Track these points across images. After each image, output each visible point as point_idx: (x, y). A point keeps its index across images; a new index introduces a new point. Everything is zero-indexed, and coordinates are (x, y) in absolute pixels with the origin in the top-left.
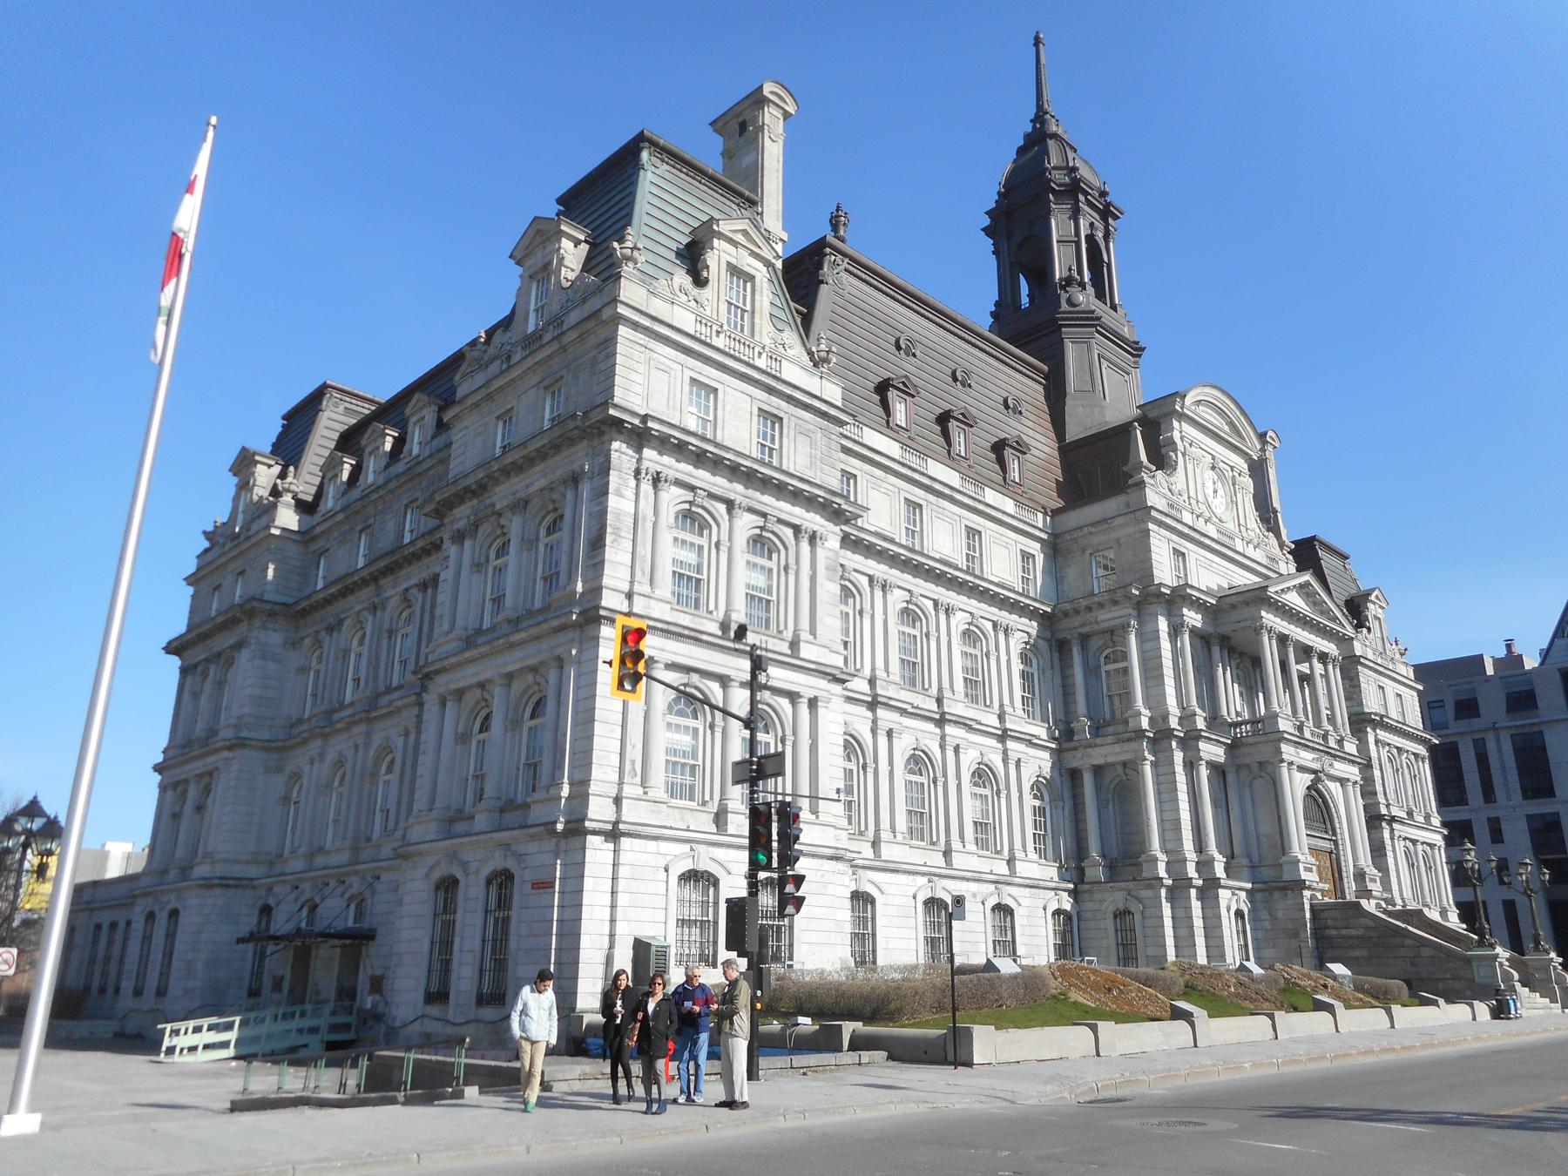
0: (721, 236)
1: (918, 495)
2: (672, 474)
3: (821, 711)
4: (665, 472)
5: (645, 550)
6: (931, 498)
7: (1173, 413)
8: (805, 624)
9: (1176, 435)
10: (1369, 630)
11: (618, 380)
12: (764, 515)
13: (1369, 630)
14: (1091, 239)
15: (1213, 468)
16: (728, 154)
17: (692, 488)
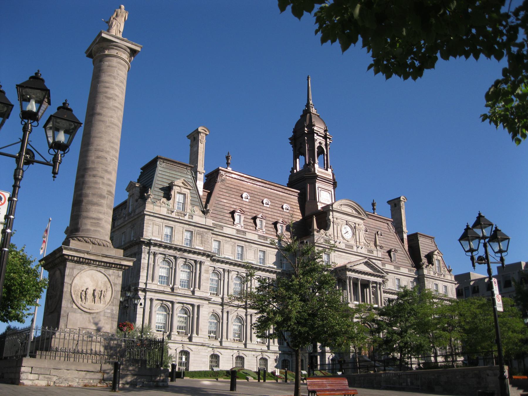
0: (175, 185)
1: (242, 244)
2: (158, 252)
3: (201, 308)
4: (156, 252)
5: (150, 272)
6: (247, 244)
7: (330, 210)
8: (197, 286)
9: (331, 217)
10: (433, 265)
11: (144, 230)
12: (186, 259)
13: (433, 265)
14: (320, 148)
15: (347, 224)
16: (192, 146)
17: (165, 255)
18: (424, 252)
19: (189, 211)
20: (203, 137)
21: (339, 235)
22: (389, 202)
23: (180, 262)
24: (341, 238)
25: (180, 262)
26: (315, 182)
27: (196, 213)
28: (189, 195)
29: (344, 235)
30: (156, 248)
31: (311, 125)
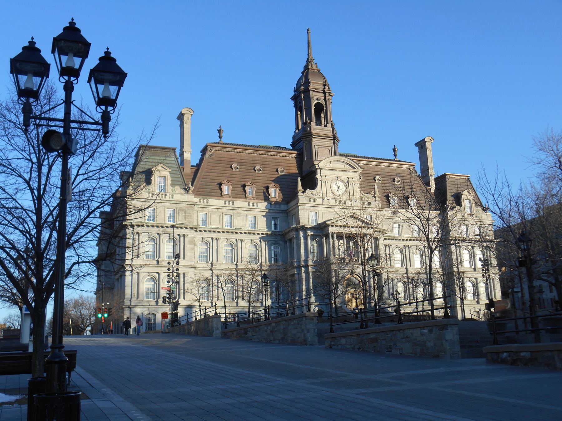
9: (318, 176)
10: (461, 206)
13: (461, 206)
18: (450, 193)
19: (170, 191)
20: (188, 119)
21: (329, 192)
22: (416, 145)
23: (165, 238)
24: (332, 195)
25: (165, 238)
26: (311, 140)
27: (177, 192)
28: (169, 177)
29: (335, 192)
30: (140, 228)
31: (307, 83)
